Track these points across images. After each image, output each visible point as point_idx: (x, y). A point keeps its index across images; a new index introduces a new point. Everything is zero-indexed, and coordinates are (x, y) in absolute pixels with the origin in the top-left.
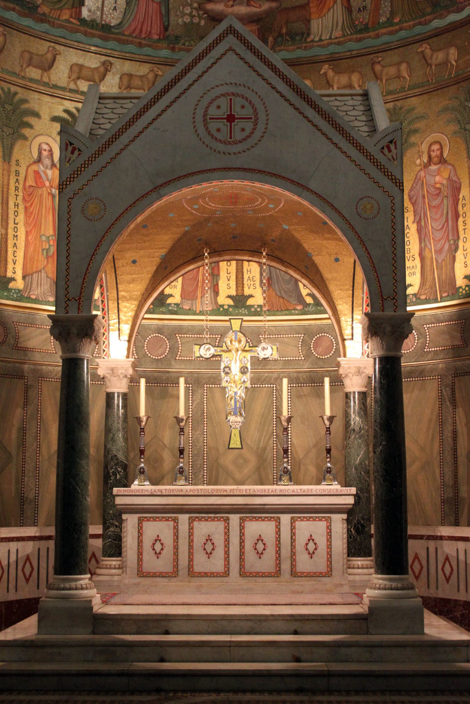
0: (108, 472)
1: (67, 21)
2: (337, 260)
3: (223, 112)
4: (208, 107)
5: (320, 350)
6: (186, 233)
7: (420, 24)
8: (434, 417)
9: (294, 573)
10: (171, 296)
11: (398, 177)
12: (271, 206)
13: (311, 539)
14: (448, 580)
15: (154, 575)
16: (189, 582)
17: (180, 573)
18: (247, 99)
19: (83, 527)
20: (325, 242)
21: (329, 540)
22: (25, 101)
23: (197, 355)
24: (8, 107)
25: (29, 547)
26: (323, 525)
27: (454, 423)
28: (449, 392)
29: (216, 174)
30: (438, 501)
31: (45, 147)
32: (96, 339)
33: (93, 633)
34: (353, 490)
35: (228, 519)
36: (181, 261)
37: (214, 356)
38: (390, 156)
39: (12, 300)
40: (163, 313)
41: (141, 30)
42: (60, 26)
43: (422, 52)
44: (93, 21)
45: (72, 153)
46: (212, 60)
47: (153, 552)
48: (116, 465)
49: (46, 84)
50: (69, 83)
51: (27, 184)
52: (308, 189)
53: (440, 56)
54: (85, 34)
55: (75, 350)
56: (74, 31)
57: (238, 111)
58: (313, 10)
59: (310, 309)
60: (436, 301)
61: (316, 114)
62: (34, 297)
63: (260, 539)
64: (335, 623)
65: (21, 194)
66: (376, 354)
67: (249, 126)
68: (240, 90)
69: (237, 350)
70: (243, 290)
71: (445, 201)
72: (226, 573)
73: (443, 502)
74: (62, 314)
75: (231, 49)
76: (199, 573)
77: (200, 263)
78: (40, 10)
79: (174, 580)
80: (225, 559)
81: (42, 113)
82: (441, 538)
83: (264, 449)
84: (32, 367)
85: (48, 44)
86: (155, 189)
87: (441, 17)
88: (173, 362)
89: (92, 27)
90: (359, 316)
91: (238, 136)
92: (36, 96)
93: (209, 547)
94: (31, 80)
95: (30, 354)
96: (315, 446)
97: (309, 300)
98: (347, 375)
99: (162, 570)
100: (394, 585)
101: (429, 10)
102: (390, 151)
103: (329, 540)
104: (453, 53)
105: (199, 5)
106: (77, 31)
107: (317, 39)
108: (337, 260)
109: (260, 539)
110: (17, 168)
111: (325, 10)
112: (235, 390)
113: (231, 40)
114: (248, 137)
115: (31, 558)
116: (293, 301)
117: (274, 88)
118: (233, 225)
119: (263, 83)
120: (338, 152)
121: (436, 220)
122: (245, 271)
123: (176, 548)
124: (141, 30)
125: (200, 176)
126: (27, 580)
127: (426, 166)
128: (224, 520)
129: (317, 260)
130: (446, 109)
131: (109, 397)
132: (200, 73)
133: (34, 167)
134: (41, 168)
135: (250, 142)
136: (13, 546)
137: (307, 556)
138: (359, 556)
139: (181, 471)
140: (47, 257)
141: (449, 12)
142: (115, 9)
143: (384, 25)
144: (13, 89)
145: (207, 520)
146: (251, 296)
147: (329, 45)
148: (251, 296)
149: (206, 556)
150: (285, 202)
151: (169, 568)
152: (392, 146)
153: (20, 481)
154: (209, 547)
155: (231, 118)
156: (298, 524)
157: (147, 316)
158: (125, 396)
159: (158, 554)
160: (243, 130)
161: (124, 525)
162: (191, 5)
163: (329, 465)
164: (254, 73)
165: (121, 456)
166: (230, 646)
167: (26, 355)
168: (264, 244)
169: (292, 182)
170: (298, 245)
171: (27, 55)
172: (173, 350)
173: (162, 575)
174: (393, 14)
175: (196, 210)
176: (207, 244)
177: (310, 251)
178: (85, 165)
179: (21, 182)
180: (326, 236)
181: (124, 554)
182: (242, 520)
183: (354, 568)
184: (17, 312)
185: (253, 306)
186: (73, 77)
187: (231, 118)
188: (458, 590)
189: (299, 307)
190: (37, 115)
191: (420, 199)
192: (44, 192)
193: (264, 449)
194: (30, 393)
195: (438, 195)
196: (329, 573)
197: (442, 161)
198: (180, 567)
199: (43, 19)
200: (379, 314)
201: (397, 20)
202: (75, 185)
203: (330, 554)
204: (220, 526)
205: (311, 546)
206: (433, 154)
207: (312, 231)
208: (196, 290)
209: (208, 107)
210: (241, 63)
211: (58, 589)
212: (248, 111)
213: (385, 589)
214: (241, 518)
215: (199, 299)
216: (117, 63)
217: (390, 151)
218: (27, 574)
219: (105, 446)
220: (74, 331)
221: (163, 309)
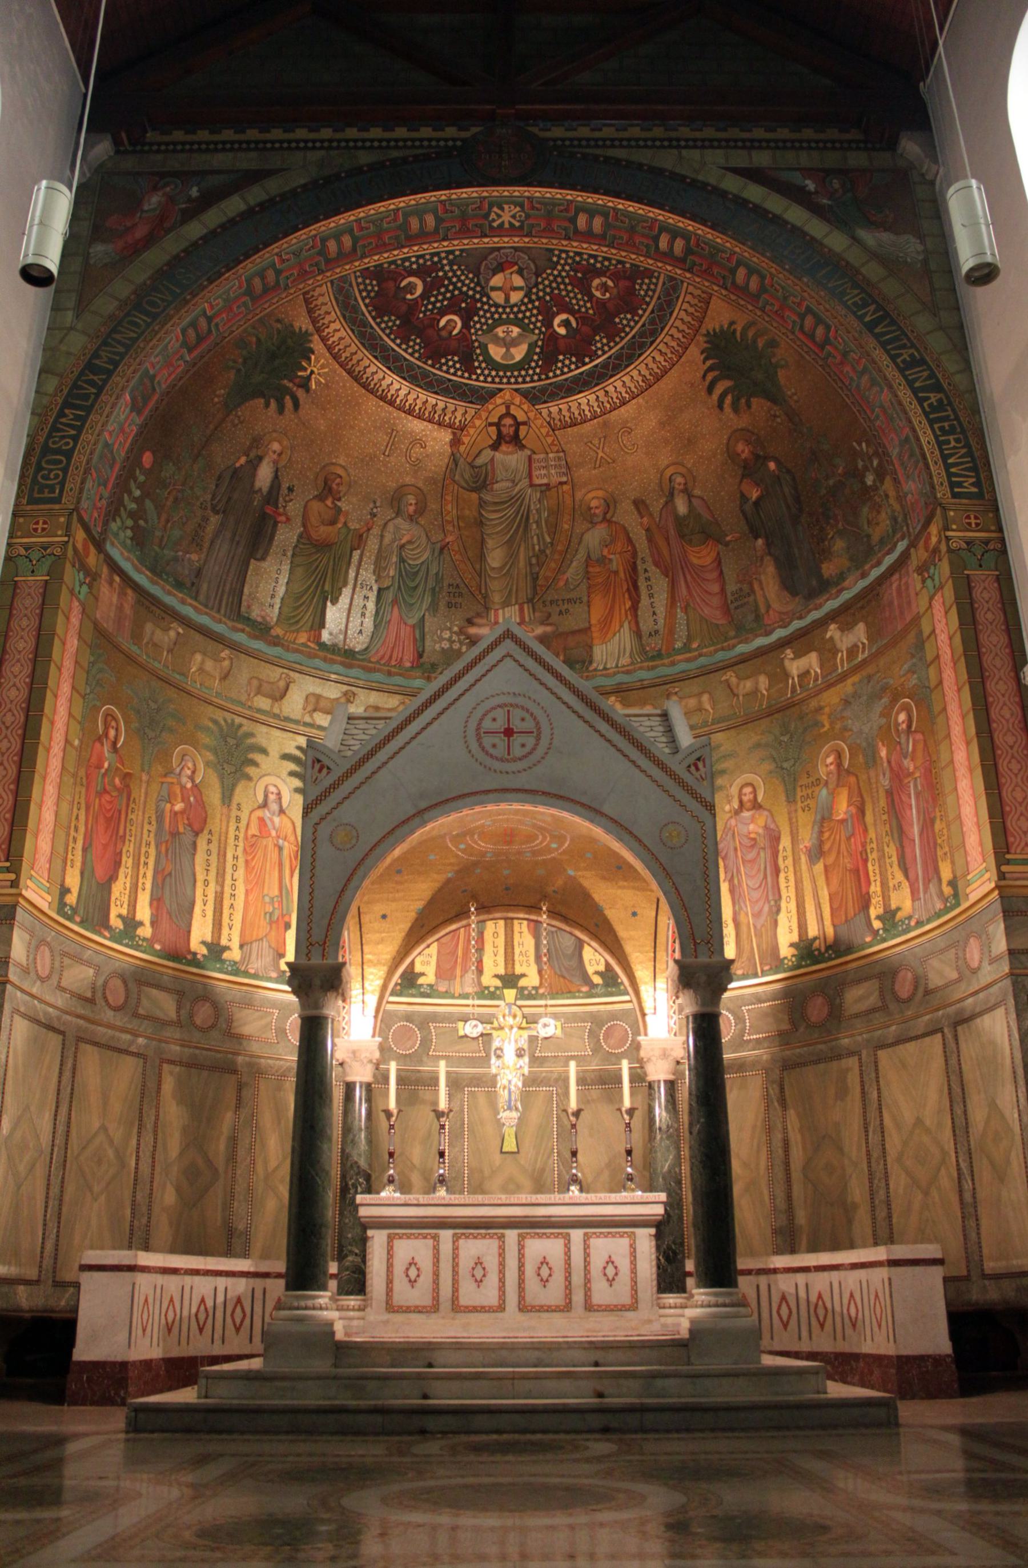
0: (347, 1185)
1: (304, 645)
2: (634, 914)
3: (500, 724)
4: (481, 719)
5: (612, 1042)
6: (448, 881)
7: (723, 649)
8: (759, 1124)
9: (589, 1307)
10: (423, 974)
11: (709, 799)
12: (554, 846)
13: (610, 1261)
14: (785, 1326)
15: (408, 1310)
16: (453, 1319)
17: (442, 1307)
18: (528, 711)
19: (323, 1229)
20: (619, 891)
21: (633, 1262)
22: (252, 735)
23: (461, 1033)
24: (232, 741)
25: (240, 1286)
26: (625, 1242)
27: (785, 1129)
28: (777, 1090)
29: (491, 796)
30: (769, 1232)
31: (272, 789)
32: (343, 995)
33: (335, 1366)
34: (663, 1196)
35: (503, 1236)
36: (441, 919)
37: (482, 1035)
38: (697, 774)
39: (226, 973)
40: (413, 996)
41: (391, 657)
42: (297, 651)
43: (727, 681)
44: (335, 645)
45: (320, 771)
46: (487, 668)
47: (406, 1280)
48: (358, 1174)
49: (276, 716)
50: (303, 716)
51: (250, 833)
52: (603, 814)
53: (748, 685)
54: (325, 660)
55: (317, 1006)
56: (311, 656)
57: (517, 724)
58: (595, 635)
59: (599, 990)
60: (755, 975)
61: (609, 728)
62: (252, 971)
63: (544, 1262)
64: (647, 1351)
65: (241, 844)
66: (689, 1010)
67: (530, 741)
68: (520, 701)
69: (512, 1027)
70: (513, 968)
71: (762, 854)
72: (501, 1308)
73: (776, 1232)
74: (304, 961)
75: (508, 655)
76: (466, 1307)
77: (464, 922)
78: (273, 632)
79: (434, 1316)
80: (500, 1289)
81: (270, 750)
82: (775, 1271)
83: (543, 1170)
84: (247, 1059)
85: (281, 670)
86: (420, 813)
87: (746, 641)
88: (425, 1059)
89: (333, 652)
90: (662, 984)
91: (517, 751)
92: (264, 729)
93: (479, 1273)
94: (259, 711)
95: (245, 1043)
96: (608, 1165)
97: (597, 980)
98: (649, 1060)
99: (418, 1303)
100: (721, 1300)
101: (732, 633)
102: (697, 769)
103: (633, 1262)
104: (763, 682)
105: (461, 629)
106: (315, 656)
107: (601, 667)
108: (634, 914)
109: (544, 1262)
110: (239, 813)
111: (609, 635)
112: (510, 1077)
113: (508, 645)
114: (530, 753)
115: (243, 1300)
116: (577, 981)
117: (559, 698)
118: (506, 872)
119: (546, 692)
120: (637, 771)
121: (752, 877)
122: (516, 943)
123: (436, 1274)
124: (391, 657)
125: (473, 798)
126: (238, 1329)
127: (737, 813)
128: (499, 1238)
129: (610, 914)
130: (758, 745)
131: (350, 1087)
132: (472, 681)
133: (259, 813)
134: (266, 814)
135: (534, 758)
136: (221, 1282)
137: (606, 1284)
138: (671, 1291)
139: (442, 1180)
140: (271, 923)
141: (757, 636)
142: (361, 632)
143: (679, 652)
144: (238, 720)
145: (475, 1238)
146: (523, 975)
147: (615, 674)
148: (523, 975)
149: (474, 1285)
150: (572, 840)
151: (427, 1301)
152: (700, 765)
153: (227, 1206)
154: (479, 1273)
155: (509, 732)
156: (593, 1242)
157: (392, 999)
158: (368, 1087)
159: (412, 1282)
160: (523, 745)
161: (369, 1244)
162: (450, 629)
163: (629, 1170)
164: (535, 682)
165: (363, 1163)
166: (513, 1379)
167: (241, 1044)
168: (545, 897)
169: (583, 805)
170: (587, 896)
171: (255, 682)
172: (426, 1043)
173: (419, 1310)
174: (690, 638)
175: (463, 851)
176: (474, 897)
177: (601, 903)
178: (334, 786)
179: (243, 830)
180: (621, 883)
181: (368, 1290)
182: (522, 1238)
183: (664, 1308)
184: (230, 989)
185: (526, 988)
186: (309, 708)
187: (509, 732)
188: (800, 1338)
189: (585, 989)
190: (264, 751)
191: (732, 853)
192: (270, 843)
193: (543, 1170)
194: (244, 1092)
195: (752, 846)
196: (633, 1306)
197: (756, 806)
198: (441, 1299)
199: (276, 642)
200: (691, 960)
201: (695, 645)
202: (322, 809)
203: (634, 1282)
204: (494, 1244)
205: (610, 1271)
206: (745, 799)
207: (603, 878)
208: (454, 968)
209: (481, 719)
210: (521, 669)
211: (291, 1308)
212: (529, 725)
213: (709, 1306)
214: (519, 1235)
215: (458, 979)
216: (362, 694)
217: (697, 769)
218: (238, 1321)
219: (343, 1151)
220: (317, 982)
221: (413, 991)
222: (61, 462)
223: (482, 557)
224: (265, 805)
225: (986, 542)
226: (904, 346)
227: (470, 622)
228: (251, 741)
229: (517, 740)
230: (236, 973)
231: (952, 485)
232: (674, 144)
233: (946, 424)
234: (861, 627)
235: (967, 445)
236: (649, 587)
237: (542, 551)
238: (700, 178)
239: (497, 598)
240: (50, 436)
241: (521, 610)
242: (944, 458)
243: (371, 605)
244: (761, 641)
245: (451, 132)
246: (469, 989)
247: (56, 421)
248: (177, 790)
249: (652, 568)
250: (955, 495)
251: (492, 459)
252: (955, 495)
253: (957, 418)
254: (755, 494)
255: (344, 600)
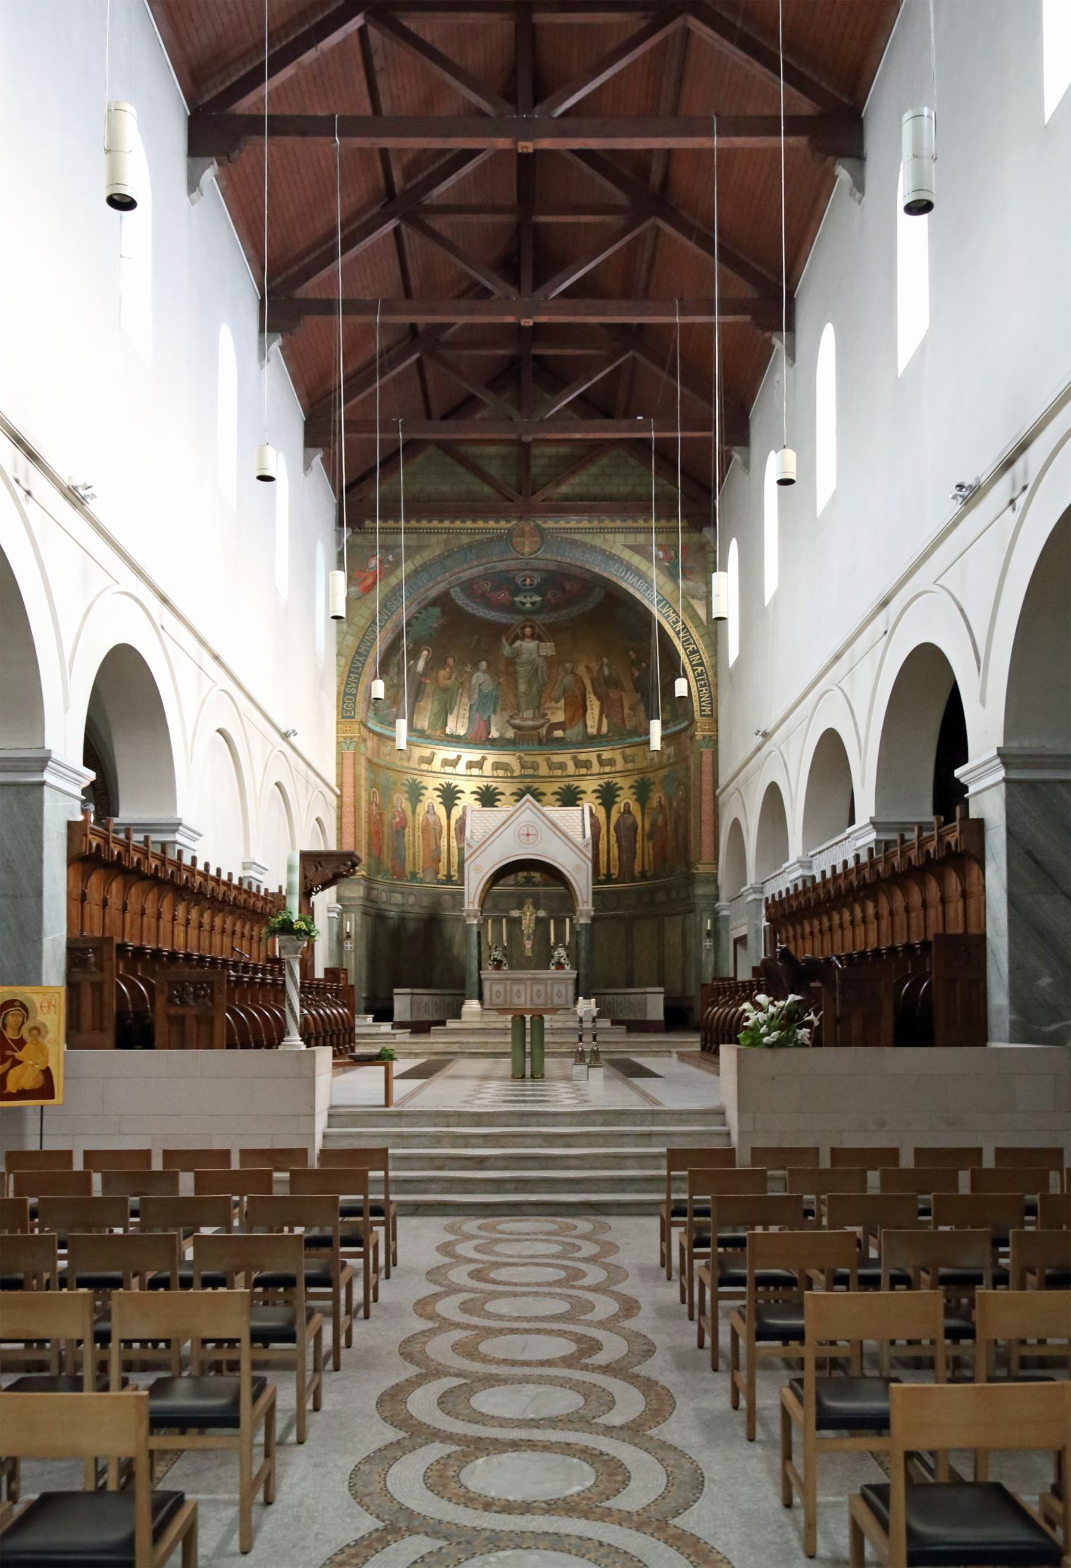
3: (525, 832)
22: (421, 782)
67: (535, 837)
94: (424, 771)
141: (635, 736)
144: (416, 777)
155: (528, 835)
187: (528, 835)
190: (426, 788)
201: (610, 735)
212: (534, 832)
222: (351, 700)
223: (517, 688)
224: (428, 812)
225: (710, 737)
226: (690, 644)
227: (511, 717)
228: (421, 785)
229: (531, 837)
230: (421, 883)
231: (702, 711)
232: (602, 530)
233: (703, 682)
234: (672, 748)
235: (710, 692)
236: (592, 705)
237: (544, 685)
238: (613, 551)
239: (523, 706)
240: (346, 687)
241: (534, 712)
242: (700, 698)
243: (467, 715)
244: (637, 739)
245: (503, 524)
246: (512, 883)
247: (347, 680)
248: (396, 813)
249: (592, 696)
250: (702, 716)
251: (521, 645)
252: (702, 716)
253: (708, 679)
254: (637, 674)
255: (455, 712)
